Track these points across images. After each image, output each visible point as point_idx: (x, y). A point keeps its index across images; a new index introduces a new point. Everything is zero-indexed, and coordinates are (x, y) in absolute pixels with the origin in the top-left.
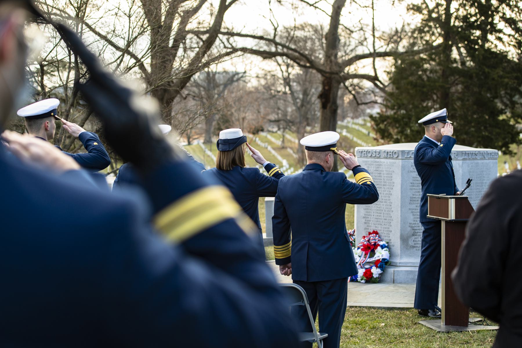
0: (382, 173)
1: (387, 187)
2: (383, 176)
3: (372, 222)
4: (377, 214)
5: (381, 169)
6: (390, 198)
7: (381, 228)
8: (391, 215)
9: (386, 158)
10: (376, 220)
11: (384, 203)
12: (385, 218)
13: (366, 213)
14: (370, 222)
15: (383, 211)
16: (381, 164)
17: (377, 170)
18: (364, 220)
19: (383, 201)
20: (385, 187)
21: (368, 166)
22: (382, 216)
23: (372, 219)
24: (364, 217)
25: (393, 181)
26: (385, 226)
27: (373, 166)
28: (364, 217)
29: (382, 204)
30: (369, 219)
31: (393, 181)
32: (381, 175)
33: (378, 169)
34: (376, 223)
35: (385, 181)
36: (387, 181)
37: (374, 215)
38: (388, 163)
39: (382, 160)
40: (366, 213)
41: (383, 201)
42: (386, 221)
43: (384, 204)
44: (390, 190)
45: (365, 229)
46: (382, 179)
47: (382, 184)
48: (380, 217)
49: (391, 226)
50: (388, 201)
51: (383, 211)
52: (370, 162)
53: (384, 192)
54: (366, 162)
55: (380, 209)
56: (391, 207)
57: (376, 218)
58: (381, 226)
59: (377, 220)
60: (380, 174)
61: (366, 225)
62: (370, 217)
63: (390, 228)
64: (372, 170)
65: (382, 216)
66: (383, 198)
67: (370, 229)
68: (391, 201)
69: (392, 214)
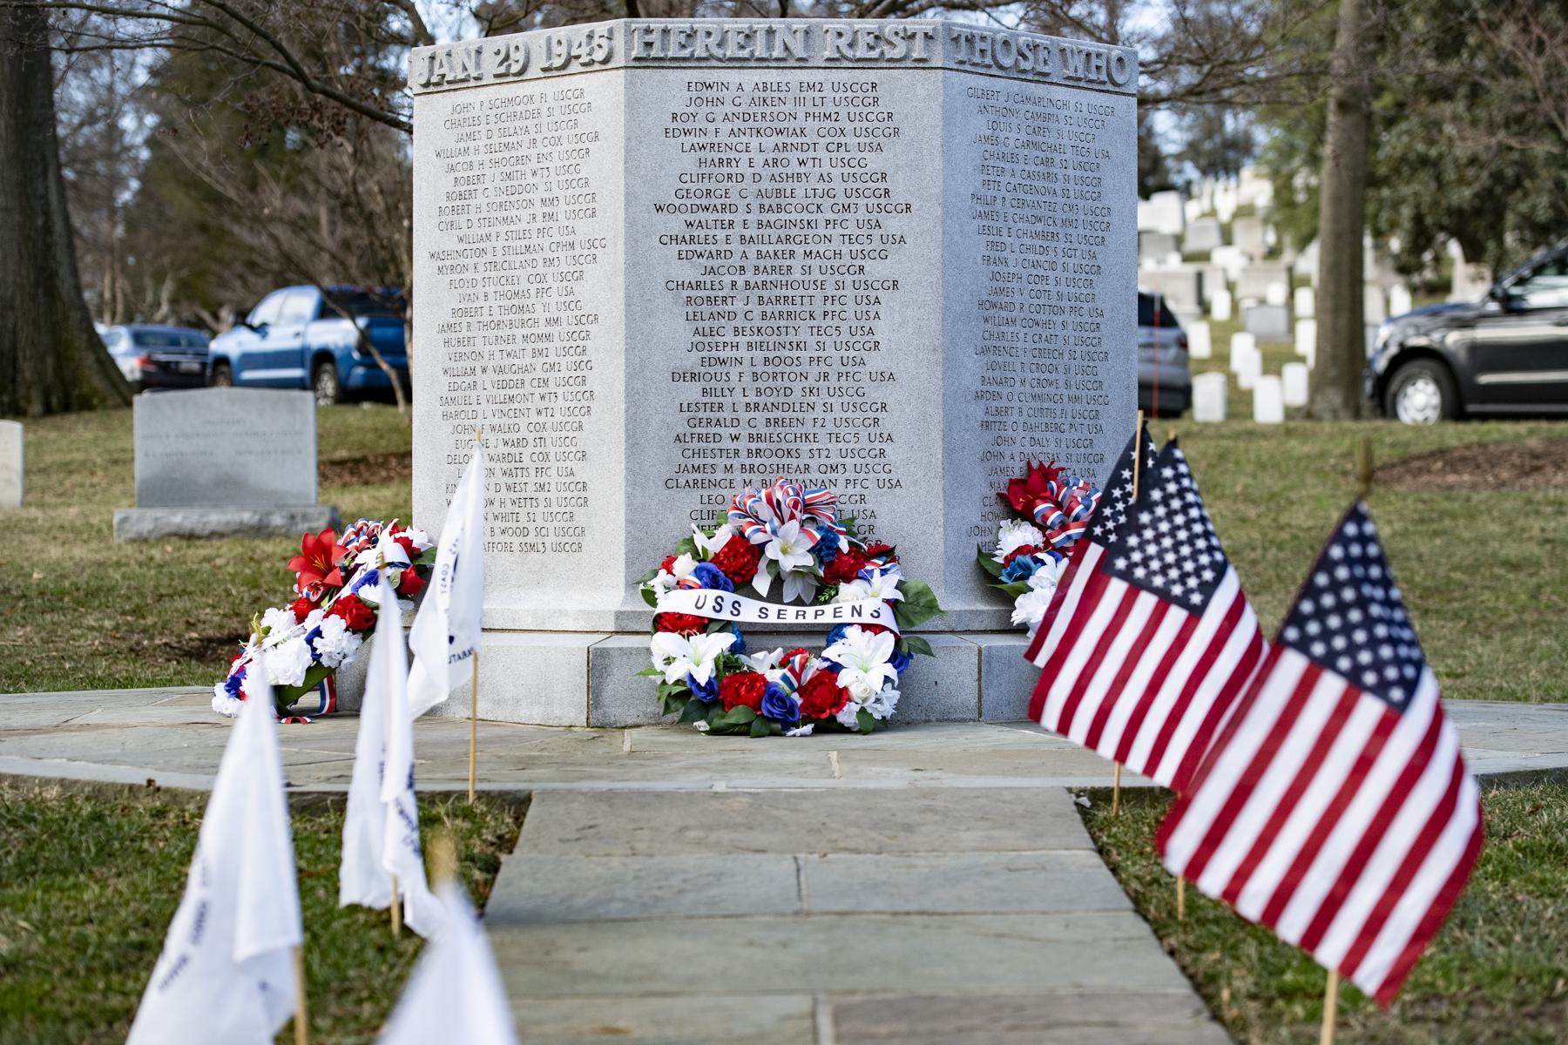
0: (1057, 158)
1: (1081, 231)
2: (1060, 177)
3: (1015, 417)
4: (1036, 375)
5: (1052, 141)
6: (1096, 291)
7: (1058, 443)
8: (1099, 378)
9: (1073, 82)
10: (1034, 404)
11: (1066, 317)
12: (1073, 392)
13: (990, 374)
14: (1009, 420)
15: (1066, 356)
16: (1054, 110)
17: (1034, 144)
18: (977, 412)
19: (1065, 303)
20: (1070, 230)
21: (993, 117)
22: (1061, 383)
23: (1016, 404)
24: (979, 396)
25: (1106, 202)
26: (1075, 435)
27: (1015, 121)
28: (979, 396)
29: (1059, 319)
30: (1004, 403)
31: (1106, 202)
32: (1051, 170)
33: (1039, 139)
34: (1032, 421)
35: (1072, 201)
36: (1081, 203)
37: (1023, 382)
38: (1084, 109)
39: (1059, 93)
40: (990, 374)
41: (1063, 304)
42: (1078, 407)
43: (1070, 318)
44: (1094, 248)
45: (987, 456)
46: (1059, 192)
47: (1059, 215)
48: (1052, 390)
49: (1099, 429)
50: (1085, 306)
51: (1066, 356)
52: (1002, 98)
53: (1066, 259)
54: (985, 94)
55: (1052, 346)
56: (1096, 334)
57: (1034, 397)
58: (1057, 434)
59: (1038, 405)
60: (1047, 162)
61: (989, 436)
62: (1005, 391)
63: (1097, 438)
64: (1011, 142)
65: (1061, 383)
66: (1062, 288)
67: (1007, 453)
68: (1099, 304)
69: (1102, 369)
